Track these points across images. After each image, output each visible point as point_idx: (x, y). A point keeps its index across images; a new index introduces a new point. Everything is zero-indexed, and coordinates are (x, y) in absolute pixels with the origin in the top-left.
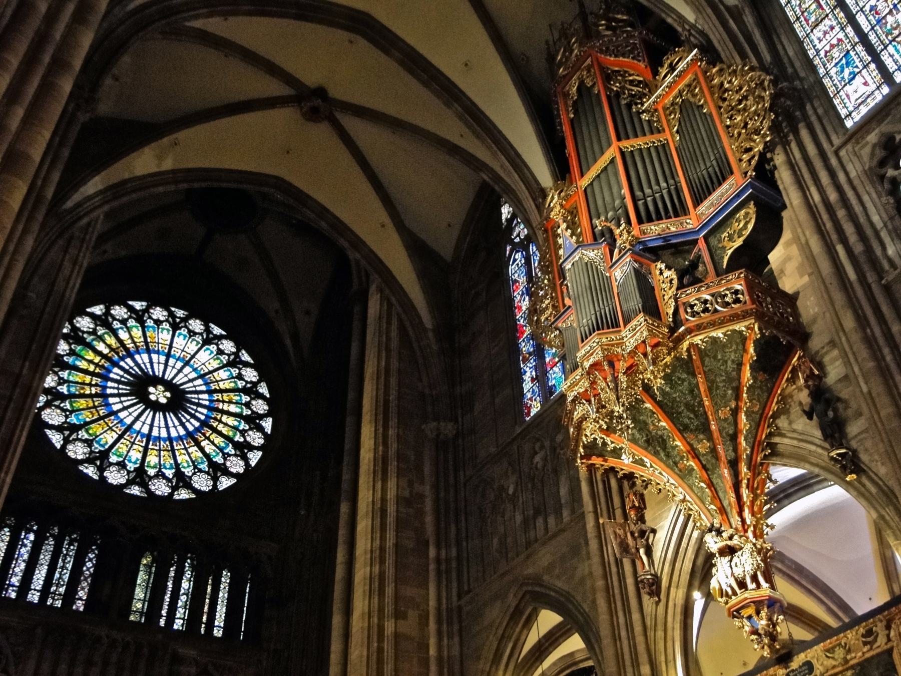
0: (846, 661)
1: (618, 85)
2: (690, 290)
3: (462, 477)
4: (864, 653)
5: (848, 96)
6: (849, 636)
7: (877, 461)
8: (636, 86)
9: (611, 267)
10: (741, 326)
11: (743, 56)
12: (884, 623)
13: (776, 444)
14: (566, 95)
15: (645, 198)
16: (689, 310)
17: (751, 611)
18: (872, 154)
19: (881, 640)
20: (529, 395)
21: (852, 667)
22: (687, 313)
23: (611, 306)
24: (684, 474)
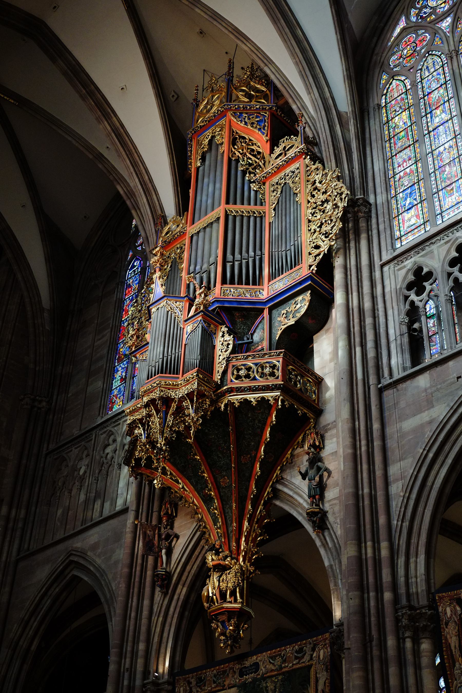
0: (281, 668)
1: (241, 151)
2: (240, 356)
3: (45, 449)
4: (293, 665)
5: (403, 221)
6: (288, 650)
7: (338, 524)
8: (253, 155)
9: (185, 321)
10: (269, 395)
11: (338, 163)
12: (312, 645)
13: (280, 490)
14: (199, 144)
15: (233, 262)
16: (235, 373)
17: (224, 618)
18: (405, 278)
19: (307, 657)
20: (116, 392)
21: (283, 673)
22: (233, 374)
23: (177, 354)
24: (208, 500)
